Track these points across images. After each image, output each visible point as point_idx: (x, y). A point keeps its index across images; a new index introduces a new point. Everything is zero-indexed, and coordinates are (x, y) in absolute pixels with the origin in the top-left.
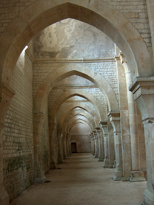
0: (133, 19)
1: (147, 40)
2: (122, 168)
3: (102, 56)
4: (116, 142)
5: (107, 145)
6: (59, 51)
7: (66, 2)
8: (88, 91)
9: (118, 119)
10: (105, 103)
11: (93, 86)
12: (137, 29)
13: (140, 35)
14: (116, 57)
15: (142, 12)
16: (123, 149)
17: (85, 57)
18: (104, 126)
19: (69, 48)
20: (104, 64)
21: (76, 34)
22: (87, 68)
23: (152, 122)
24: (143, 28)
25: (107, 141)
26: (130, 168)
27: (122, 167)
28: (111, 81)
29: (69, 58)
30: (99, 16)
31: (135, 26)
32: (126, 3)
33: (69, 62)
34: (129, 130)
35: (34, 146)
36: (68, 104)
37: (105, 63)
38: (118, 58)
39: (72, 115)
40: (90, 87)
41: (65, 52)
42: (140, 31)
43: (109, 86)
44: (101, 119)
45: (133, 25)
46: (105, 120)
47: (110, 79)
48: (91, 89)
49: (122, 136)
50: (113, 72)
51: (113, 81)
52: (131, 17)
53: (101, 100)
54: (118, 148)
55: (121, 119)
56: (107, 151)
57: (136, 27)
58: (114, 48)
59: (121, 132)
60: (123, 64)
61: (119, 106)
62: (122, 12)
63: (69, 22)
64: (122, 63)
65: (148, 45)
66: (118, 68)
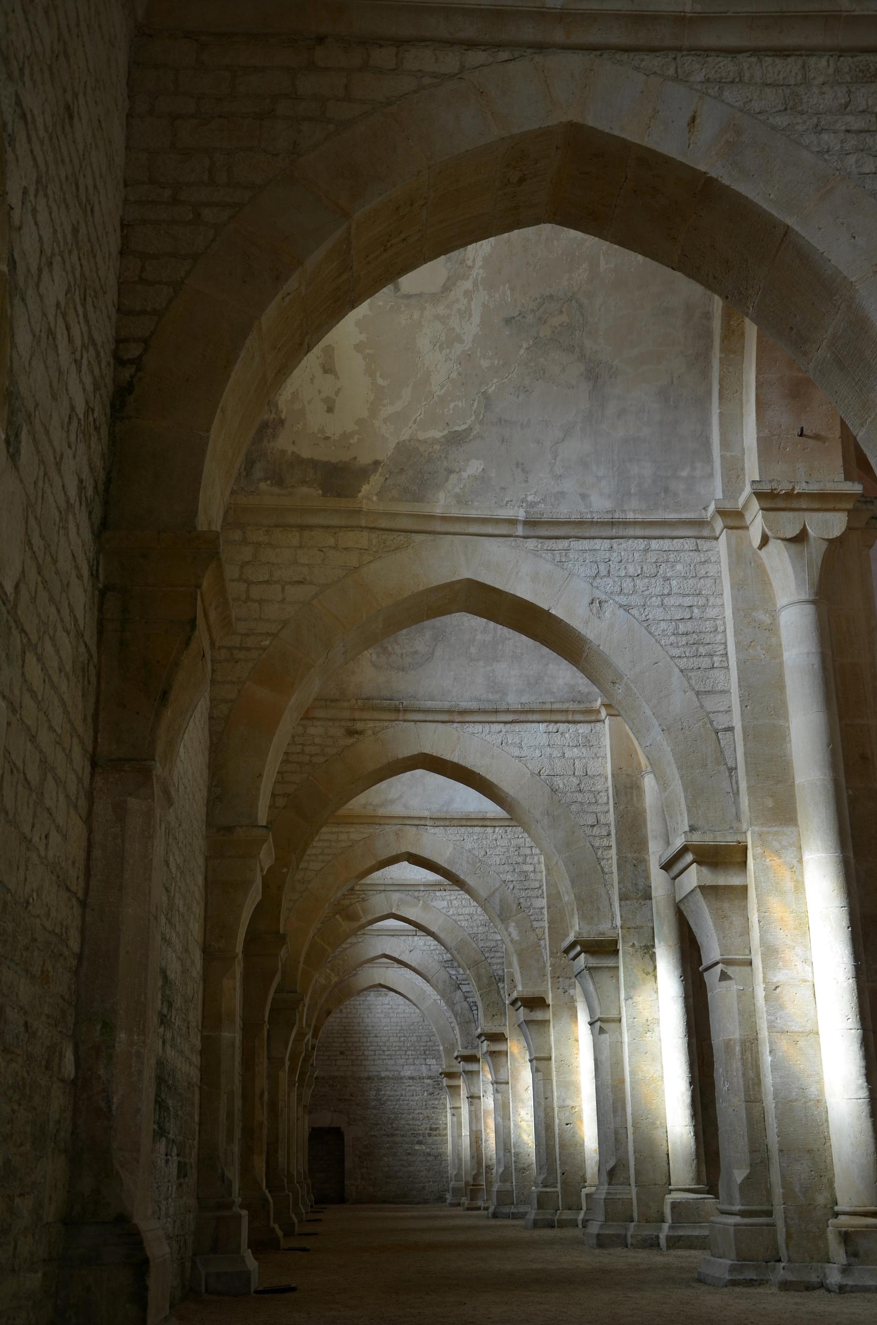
3: (634, 503)
6: (377, 463)
7: (564, 119)
10: (603, 820)
11: (532, 712)
14: (722, 513)
17: (533, 505)
20: (646, 550)
21: (485, 363)
29: (441, 503)
30: (741, 210)
33: (438, 527)
35: (204, 1039)
36: (343, 837)
37: (654, 544)
38: (734, 519)
39: (352, 917)
40: (510, 718)
41: (416, 470)
43: (676, 678)
44: (576, 920)
48: (517, 727)
51: (702, 650)
53: (579, 797)
58: (709, 459)
60: (763, 553)
61: (736, 803)
63: (446, 288)
64: (756, 541)
66: (732, 577)
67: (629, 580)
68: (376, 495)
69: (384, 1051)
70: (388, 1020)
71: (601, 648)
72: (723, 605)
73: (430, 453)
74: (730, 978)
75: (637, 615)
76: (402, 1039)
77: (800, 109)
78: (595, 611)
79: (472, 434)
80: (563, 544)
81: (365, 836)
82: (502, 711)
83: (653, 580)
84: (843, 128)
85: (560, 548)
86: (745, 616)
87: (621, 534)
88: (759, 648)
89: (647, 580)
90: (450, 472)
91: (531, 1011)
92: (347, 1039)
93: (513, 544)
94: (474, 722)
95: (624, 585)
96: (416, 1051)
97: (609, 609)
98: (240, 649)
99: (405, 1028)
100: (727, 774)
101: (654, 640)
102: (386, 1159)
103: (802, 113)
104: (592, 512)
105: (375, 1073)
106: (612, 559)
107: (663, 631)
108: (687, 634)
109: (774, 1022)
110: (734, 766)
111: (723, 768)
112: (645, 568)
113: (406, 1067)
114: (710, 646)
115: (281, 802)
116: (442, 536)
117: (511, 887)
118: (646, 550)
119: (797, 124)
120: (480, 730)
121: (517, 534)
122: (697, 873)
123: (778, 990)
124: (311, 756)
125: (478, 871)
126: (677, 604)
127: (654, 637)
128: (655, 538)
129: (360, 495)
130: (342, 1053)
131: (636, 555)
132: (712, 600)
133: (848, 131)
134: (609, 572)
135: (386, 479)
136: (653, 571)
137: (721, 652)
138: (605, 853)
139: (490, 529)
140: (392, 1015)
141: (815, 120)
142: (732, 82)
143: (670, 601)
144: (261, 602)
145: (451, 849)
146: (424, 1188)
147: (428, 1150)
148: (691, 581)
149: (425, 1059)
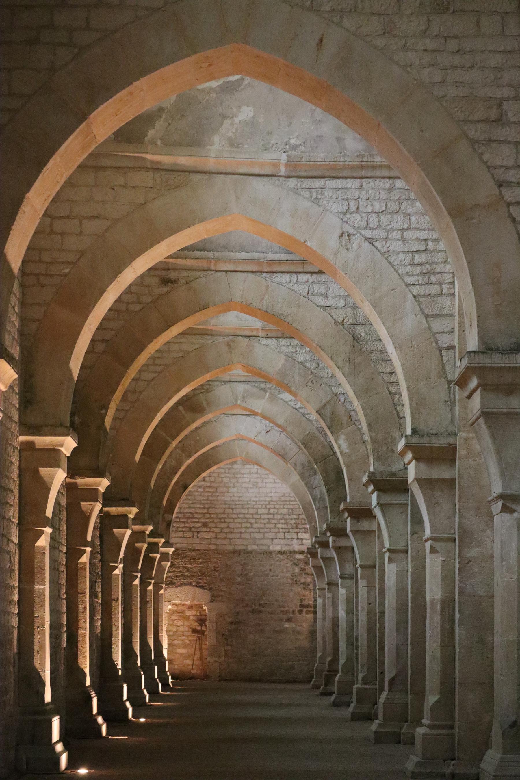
0: (479, 126)
2: (453, 718)
4: (433, 592)
6: (161, 110)
8: (303, 289)
9: (441, 472)
12: (488, 167)
17: (295, 147)
18: (387, 498)
20: (391, 189)
22: (307, 204)
24: (511, 163)
27: (453, 712)
31: (482, 154)
32: (457, 60)
42: (499, 173)
43: (410, 304)
45: (474, 149)
47: (418, 270)
49: (457, 560)
51: (433, 279)
54: (437, 619)
55: (459, 474)
56: (398, 648)
61: (452, 410)
62: (441, 94)
67: (374, 216)
68: (161, 139)
69: (251, 524)
73: (208, 100)
74: (437, 552)
75: (379, 248)
76: (272, 511)
79: (244, 84)
80: (319, 183)
81: (197, 346)
83: (395, 216)
85: (317, 186)
87: (369, 174)
89: (389, 216)
90: (225, 117)
91: (358, 521)
92: (211, 511)
94: (282, 272)
95: (370, 220)
96: (286, 523)
97: (356, 240)
98: (46, 275)
99: (275, 499)
100: (447, 386)
101: (392, 269)
102: (251, 637)
103: (395, 36)
106: (361, 196)
107: (401, 261)
108: (421, 265)
111: (443, 381)
112: (389, 204)
113: (276, 541)
115: (100, 347)
117: (342, 399)
120: (288, 280)
122: (416, 468)
123: (470, 563)
124: (128, 304)
126: (414, 237)
127: (393, 266)
129: (146, 139)
130: (205, 525)
131: (382, 193)
134: (358, 208)
135: (169, 124)
137: (449, 281)
140: (260, 485)
141: (404, 41)
142: (350, 12)
143: (408, 235)
144: (62, 234)
145: (283, 361)
146: (293, 667)
149: (297, 533)
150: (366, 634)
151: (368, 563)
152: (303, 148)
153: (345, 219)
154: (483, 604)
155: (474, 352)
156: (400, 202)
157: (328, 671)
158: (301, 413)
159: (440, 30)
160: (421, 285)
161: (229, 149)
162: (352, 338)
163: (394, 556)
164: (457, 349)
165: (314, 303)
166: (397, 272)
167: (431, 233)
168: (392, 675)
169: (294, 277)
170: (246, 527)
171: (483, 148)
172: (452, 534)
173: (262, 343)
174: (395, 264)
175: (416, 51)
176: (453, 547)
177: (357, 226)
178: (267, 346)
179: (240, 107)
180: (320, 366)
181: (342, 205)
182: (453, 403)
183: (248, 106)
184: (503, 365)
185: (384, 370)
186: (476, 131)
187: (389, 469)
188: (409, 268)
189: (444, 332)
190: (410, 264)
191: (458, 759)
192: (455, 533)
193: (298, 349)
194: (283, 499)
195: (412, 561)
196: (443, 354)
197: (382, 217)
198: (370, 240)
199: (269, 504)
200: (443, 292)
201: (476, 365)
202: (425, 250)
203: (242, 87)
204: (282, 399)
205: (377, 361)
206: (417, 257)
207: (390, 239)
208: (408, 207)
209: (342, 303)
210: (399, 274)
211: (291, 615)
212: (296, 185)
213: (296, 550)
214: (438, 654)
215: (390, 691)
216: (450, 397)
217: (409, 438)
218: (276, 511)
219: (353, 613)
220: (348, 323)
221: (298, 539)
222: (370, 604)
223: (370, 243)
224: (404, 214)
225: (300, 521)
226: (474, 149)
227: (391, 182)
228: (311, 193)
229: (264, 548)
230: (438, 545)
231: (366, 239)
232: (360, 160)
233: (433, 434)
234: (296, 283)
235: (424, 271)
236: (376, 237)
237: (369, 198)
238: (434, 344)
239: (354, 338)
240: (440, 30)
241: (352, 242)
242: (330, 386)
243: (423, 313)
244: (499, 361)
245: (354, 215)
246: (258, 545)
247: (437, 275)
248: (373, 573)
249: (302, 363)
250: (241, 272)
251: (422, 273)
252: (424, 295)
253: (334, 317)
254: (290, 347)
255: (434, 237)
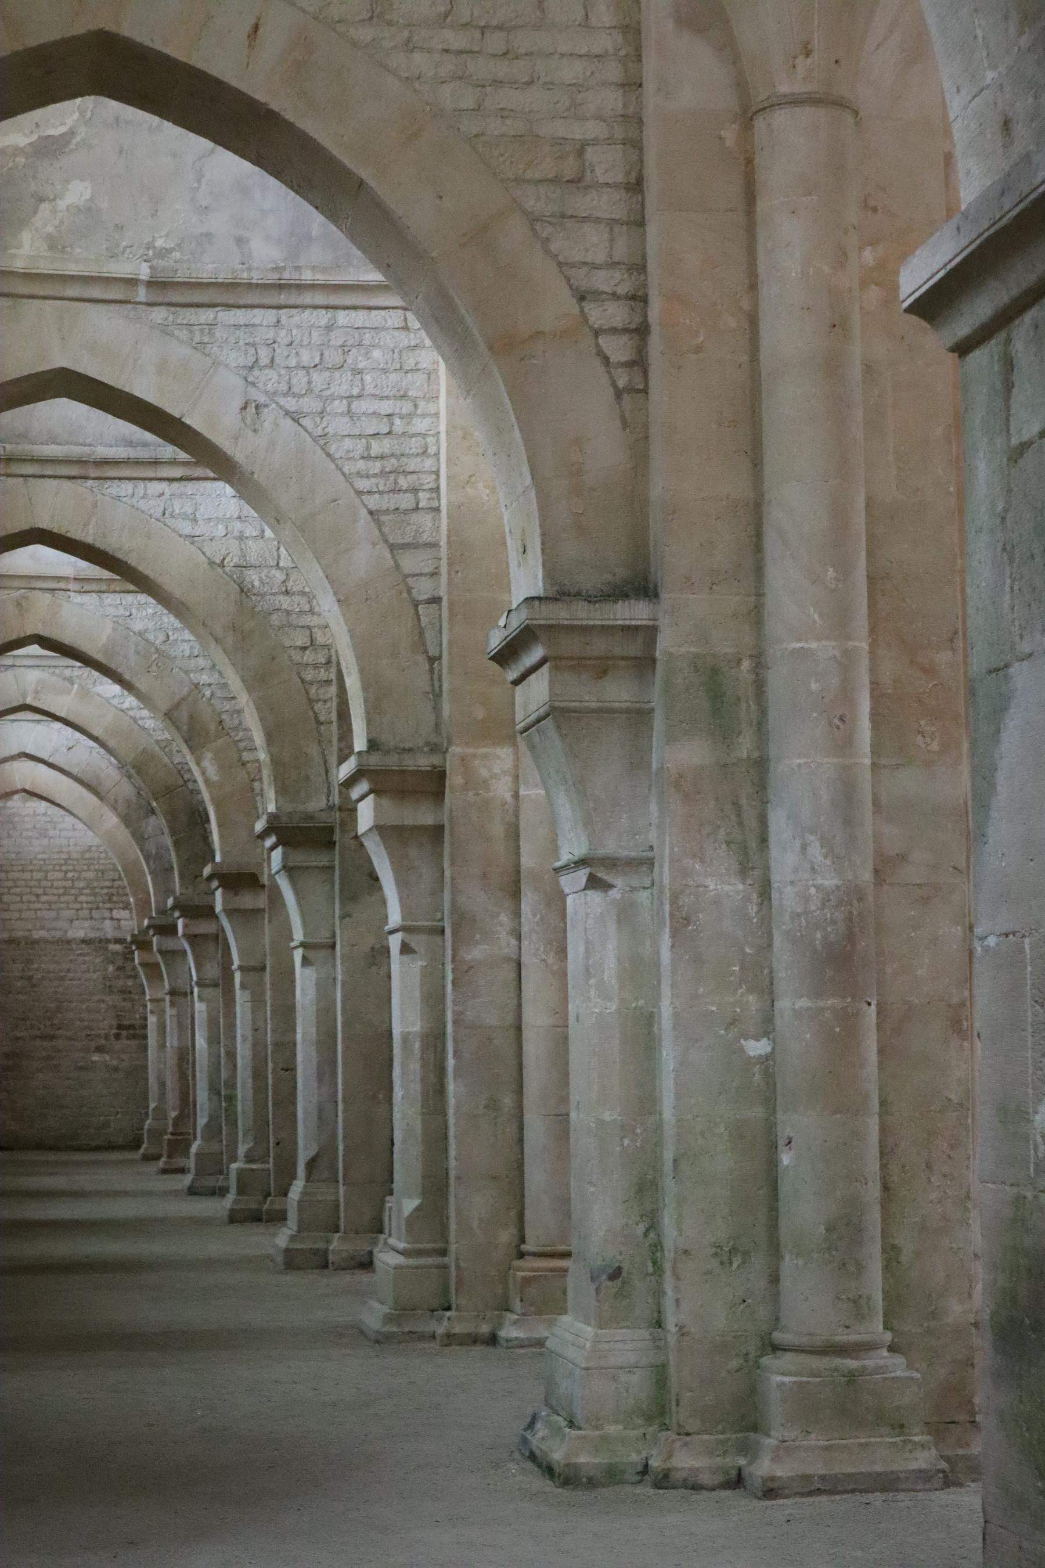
1: (619, 349)
2: (444, 1237)
4: (405, 1019)
5: (326, 1041)
7: (92, 27)
8: (155, 507)
12: (560, 264)
13: (576, 310)
15: (610, 141)
16: (458, 1073)
18: (300, 858)
19: (21, 160)
20: (329, 328)
22: (185, 351)
23: (611, 886)
24: (601, 258)
25: (325, 1013)
26: (506, 1236)
28: (381, 481)
32: (502, 69)
34: (517, 913)
44: (271, 794)
45: (534, 230)
46: (316, 804)
47: (376, 467)
48: (190, 487)
49: (449, 967)
50: (406, 407)
51: (403, 482)
52: (529, 175)
53: (285, 602)
54: (415, 1066)
56: (320, 1110)
57: (554, 247)
59: (443, 932)
61: (437, 709)
62: (475, 130)
65: (621, 383)
67: (301, 373)
69: (38, 896)
70: (45, 841)
71: (256, 476)
72: (437, 415)
76: (70, 875)
77: (388, 17)
78: (248, 420)
79: (74, 141)
80: (206, 315)
82: (166, 462)
83: (337, 374)
84: (440, 47)
85: (202, 321)
86: (464, 438)
88: (480, 485)
89: (327, 374)
90: (41, 200)
91: (236, 894)
93: (132, 314)
94: (120, 479)
95: (294, 381)
96: (95, 895)
97: (269, 415)
99: (74, 856)
100: (427, 667)
101: (333, 466)
102: (41, 1076)
103: (390, 24)
104: (249, 269)
105: (20, 934)
106: (279, 340)
107: (348, 451)
109: (462, 1013)
110: (437, 654)
111: (421, 659)
112: (326, 354)
114: (415, 476)
116: (24, 301)
117: (208, 693)
118: (329, 328)
119: (383, 38)
120: (130, 492)
121: (138, 299)
123: (473, 970)
125: (154, 668)
126: (370, 411)
128: (345, 308)
131: (315, 334)
132: (422, 404)
133: (447, 51)
134: (272, 361)
136: (338, 359)
137: (430, 486)
138: (322, 691)
139: (96, 292)
140: (51, 833)
141: (406, 33)
146: (106, 1125)
147: (115, 1063)
148: (393, 377)
149: (111, 910)
150: (250, 1081)
151: (252, 963)
152: (177, 255)
153: (251, 379)
154: (495, 1042)
155: (539, 599)
156: (346, 349)
157: (172, 1134)
158: (131, 717)
159: (472, 15)
160: (381, 493)
161: (48, 254)
162: (239, 590)
163: (312, 954)
164: (445, 603)
165: (174, 531)
166: (340, 469)
167: (399, 403)
168: (312, 1153)
169: (141, 485)
170: (29, 902)
171: (550, 229)
172: (439, 921)
173: (75, 601)
174: (337, 456)
175: (430, 51)
176: (440, 943)
177: (272, 390)
178: (82, 605)
179: (68, 182)
180: (171, 638)
181: (246, 354)
182: (438, 695)
183: (82, 180)
184: (591, 623)
185: (292, 643)
186: (538, 199)
187: (301, 808)
188: (361, 465)
189: (421, 574)
190: (363, 458)
191: (458, 1309)
192: (442, 919)
193: (134, 611)
194: (87, 855)
195: (342, 963)
196: (420, 612)
197: (315, 376)
198: (294, 415)
199: (66, 864)
200: (421, 505)
201: (543, 622)
202: (389, 433)
203: (72, 146)
204: (99, 695)
205: (282, 627)
206: (374, 444)
207: (329, 414)
208: (360, 358)
209: (221, 530)
210: (344, 474)
211: (103, 1042)
212: (166, 319)
213: (109, 937)
214: (419, 1129)
215: (308, 1179)
216: (433, 685)
217: (365, 756)
218: (76, 875)
219: (219, 1043)
220: (232, 564)
221: (112, 919)
222: (257, 1030)
223: (293, 419)
224: (353, 370)
225: (114, 891)
226: (534, 230)
227: (329, 315)
228: (191, 332)
229: (58, 934)
230: (414, 941)
231: (287, 413)
232: (276, 276)
233: (404, 749)
234: (143, 497)
235: (387, 470)
236: (305, 410)
237: (291, 344)
238: (405, 595)
239: (242, 591)
240: (472, 15)
241: (262, 419)
242: (186, 672)
243: (386, 541)
244: (584, 616)
245: (266, 371)
246: (48, 930)
247: (409, 477)
248: (262, 979)
249: (140, 634)
250: (50, 477)
251: (383, 473)
252: (388, 510)
253: (208, 553)
254: (121, 608)
255: (404, 411)
